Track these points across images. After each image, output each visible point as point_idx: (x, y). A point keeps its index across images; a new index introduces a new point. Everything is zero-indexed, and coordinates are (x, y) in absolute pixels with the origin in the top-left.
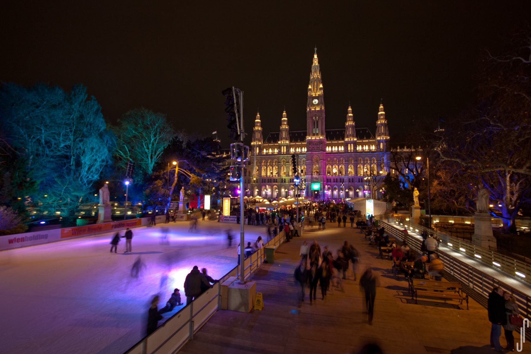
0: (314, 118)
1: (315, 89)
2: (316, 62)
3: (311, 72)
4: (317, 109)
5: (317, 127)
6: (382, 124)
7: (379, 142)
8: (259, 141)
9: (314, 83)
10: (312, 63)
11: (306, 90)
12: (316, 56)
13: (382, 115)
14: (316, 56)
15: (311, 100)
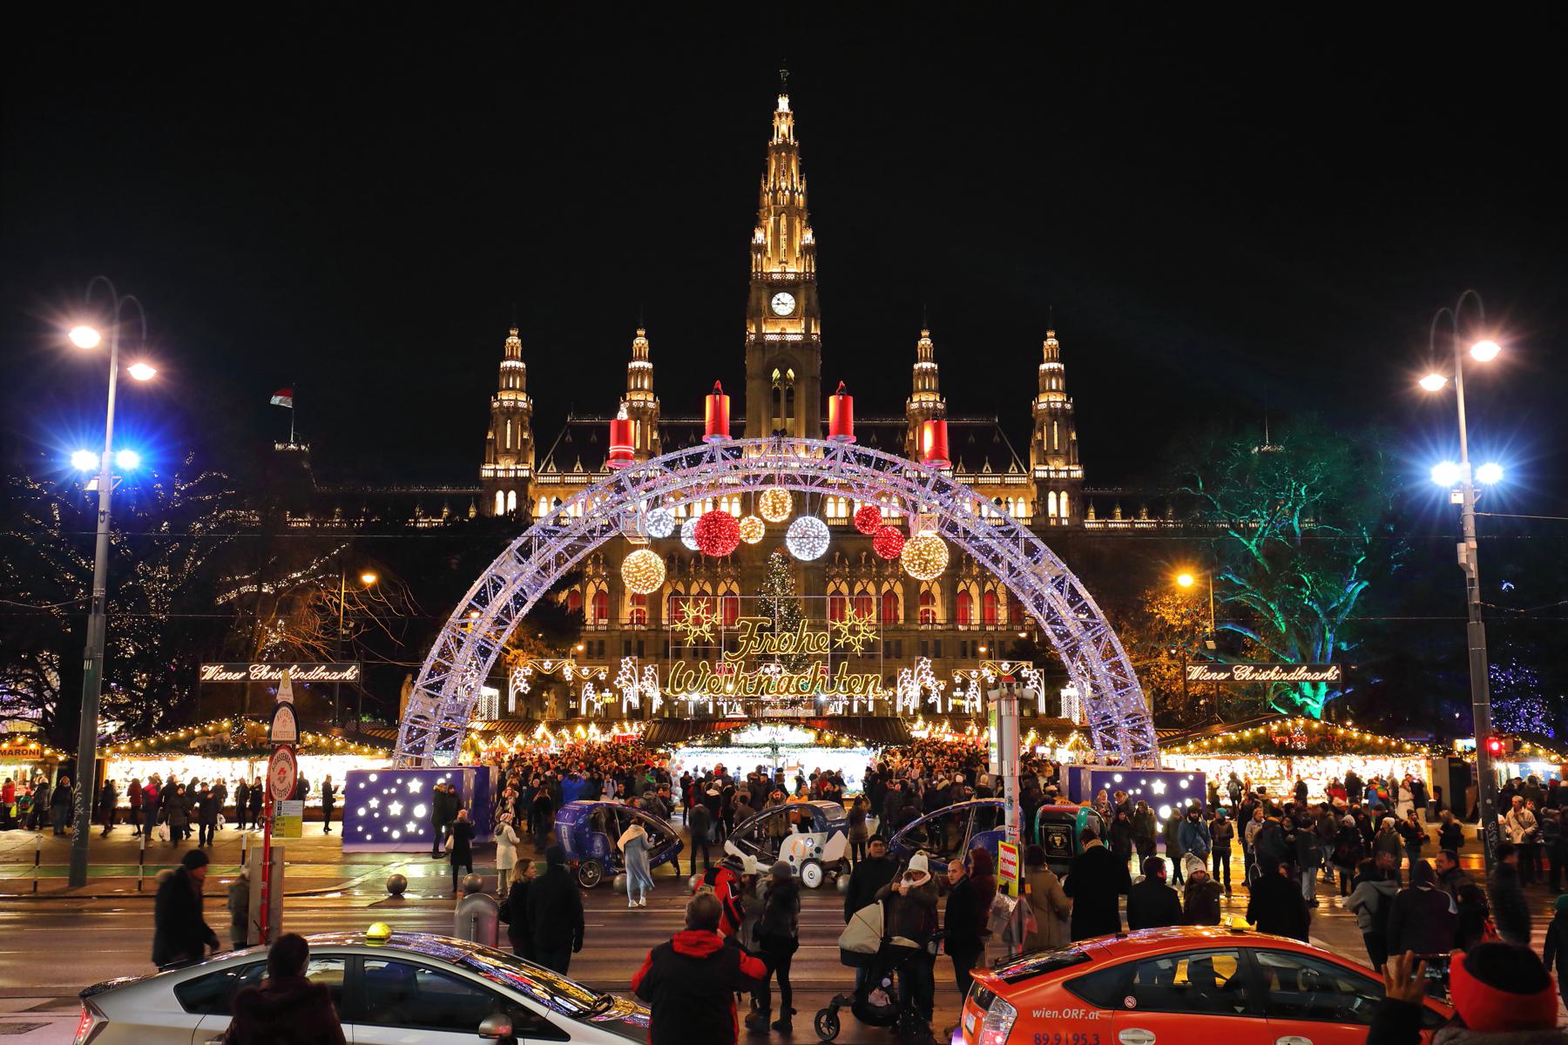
0: (776, 374)
1: (783, 244)
2: (783, 127)
3: (766, 170)
4: (789, 338)
5: (790, 414)
6: (1053, 414)
7: (1044, 486)
8: (521, 460)
9: (777, 223)
10: (770, 131)
11: (745, 249)
12: (783, 103)
13: (1052, 373)
14: (783, 103)
15: (765, 295)
